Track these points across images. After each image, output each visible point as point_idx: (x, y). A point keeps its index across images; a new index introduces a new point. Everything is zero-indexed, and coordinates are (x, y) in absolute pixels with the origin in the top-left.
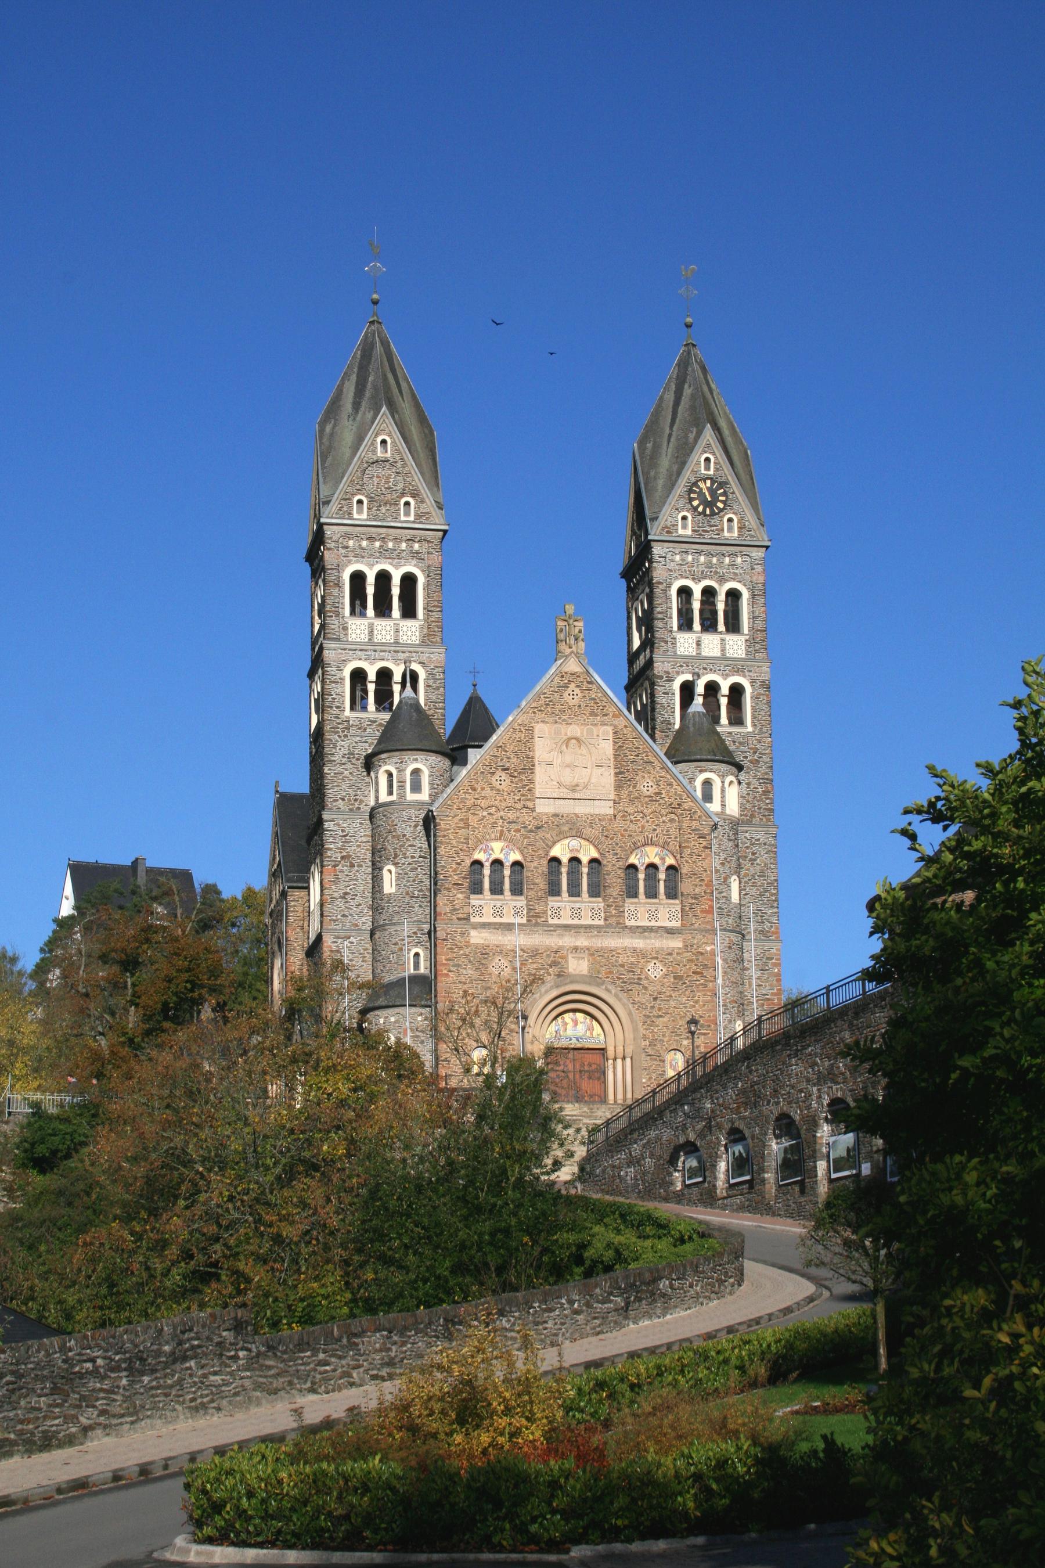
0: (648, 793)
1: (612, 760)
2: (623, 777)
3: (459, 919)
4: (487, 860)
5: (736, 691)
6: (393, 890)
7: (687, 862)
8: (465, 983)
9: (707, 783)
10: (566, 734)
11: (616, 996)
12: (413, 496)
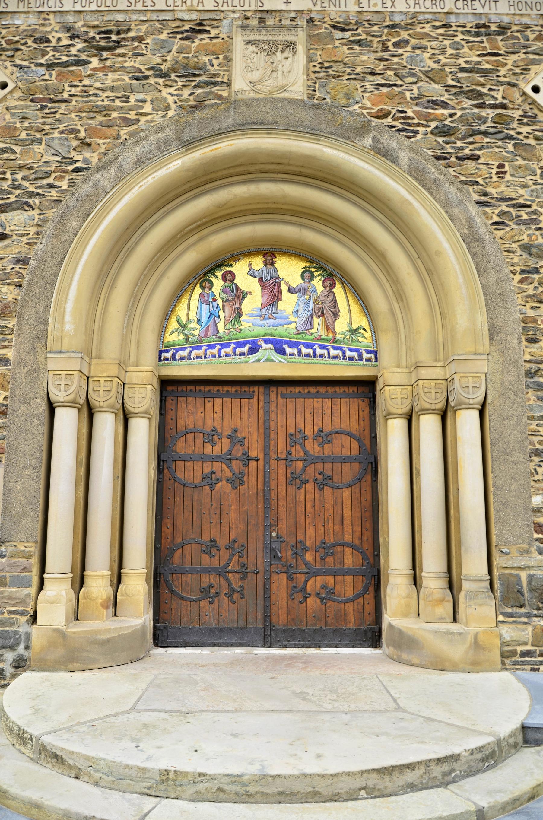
11: (417, 173)
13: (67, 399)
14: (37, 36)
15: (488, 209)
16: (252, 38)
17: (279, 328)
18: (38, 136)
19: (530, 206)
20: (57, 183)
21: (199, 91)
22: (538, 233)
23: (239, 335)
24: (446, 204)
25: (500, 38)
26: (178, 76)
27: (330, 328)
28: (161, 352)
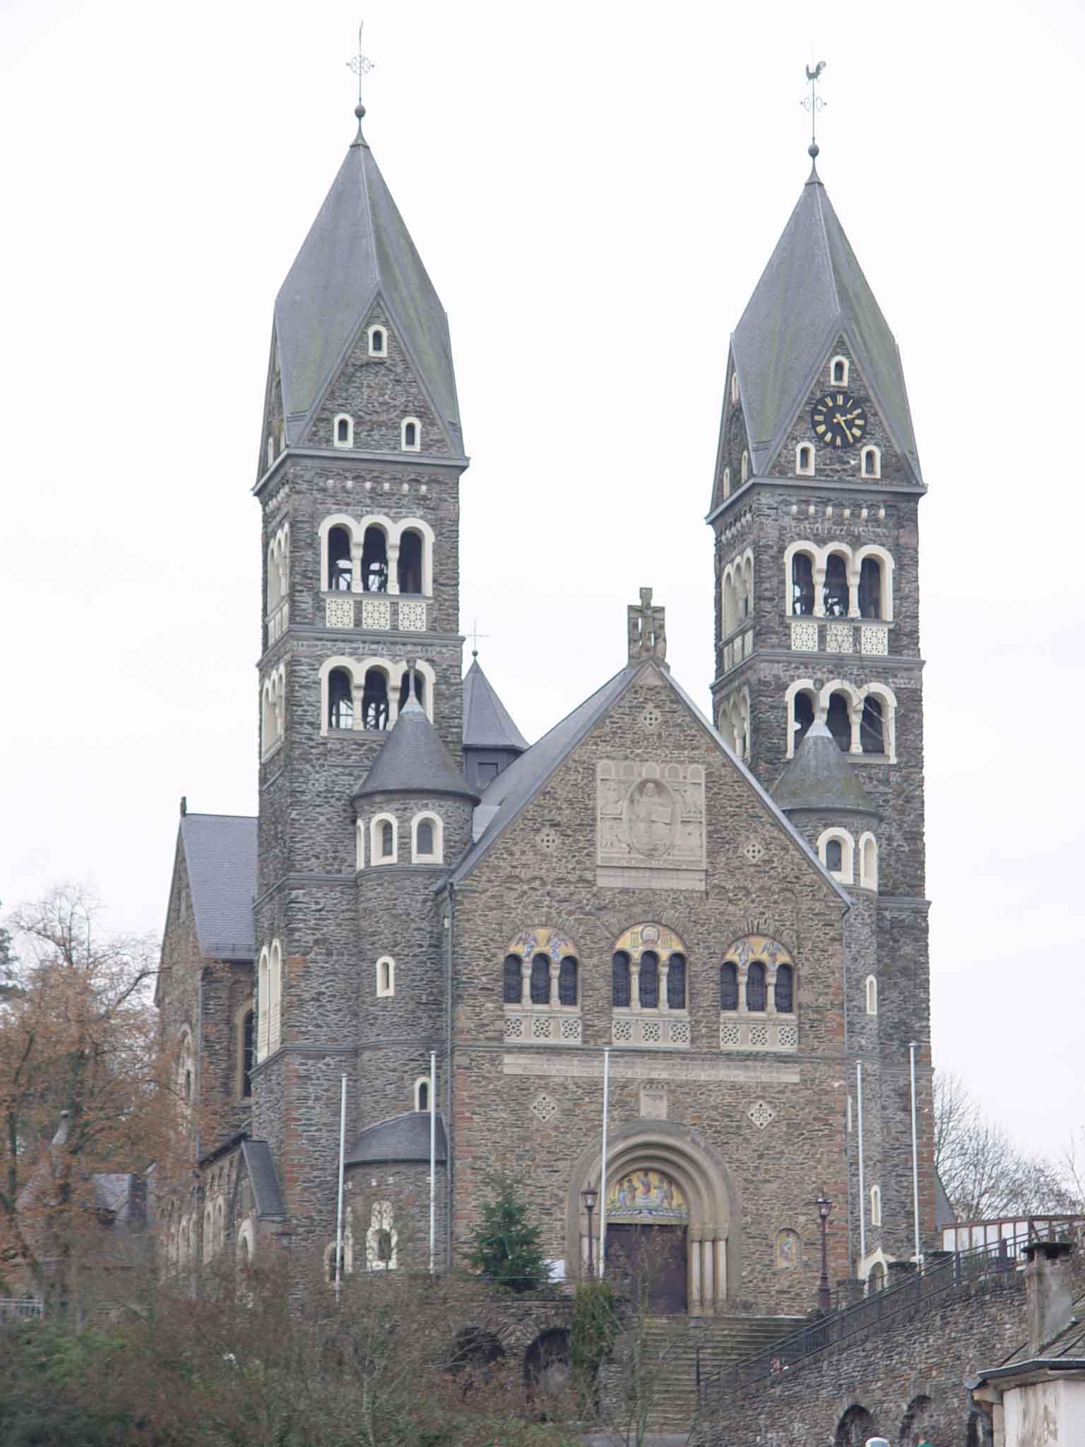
0: (754, 861)
1: (704, 812)
2: (719, 840)
3: (488, 1039)
4: (528, 954)
5: (874, 705)
6: (391, 992)
7: (807, 960)
8: (496, 1132)
9: (835, 845)
10: (640, 775)
11: (706, 1150)
12: (420, 416)
27: (670, 1204)
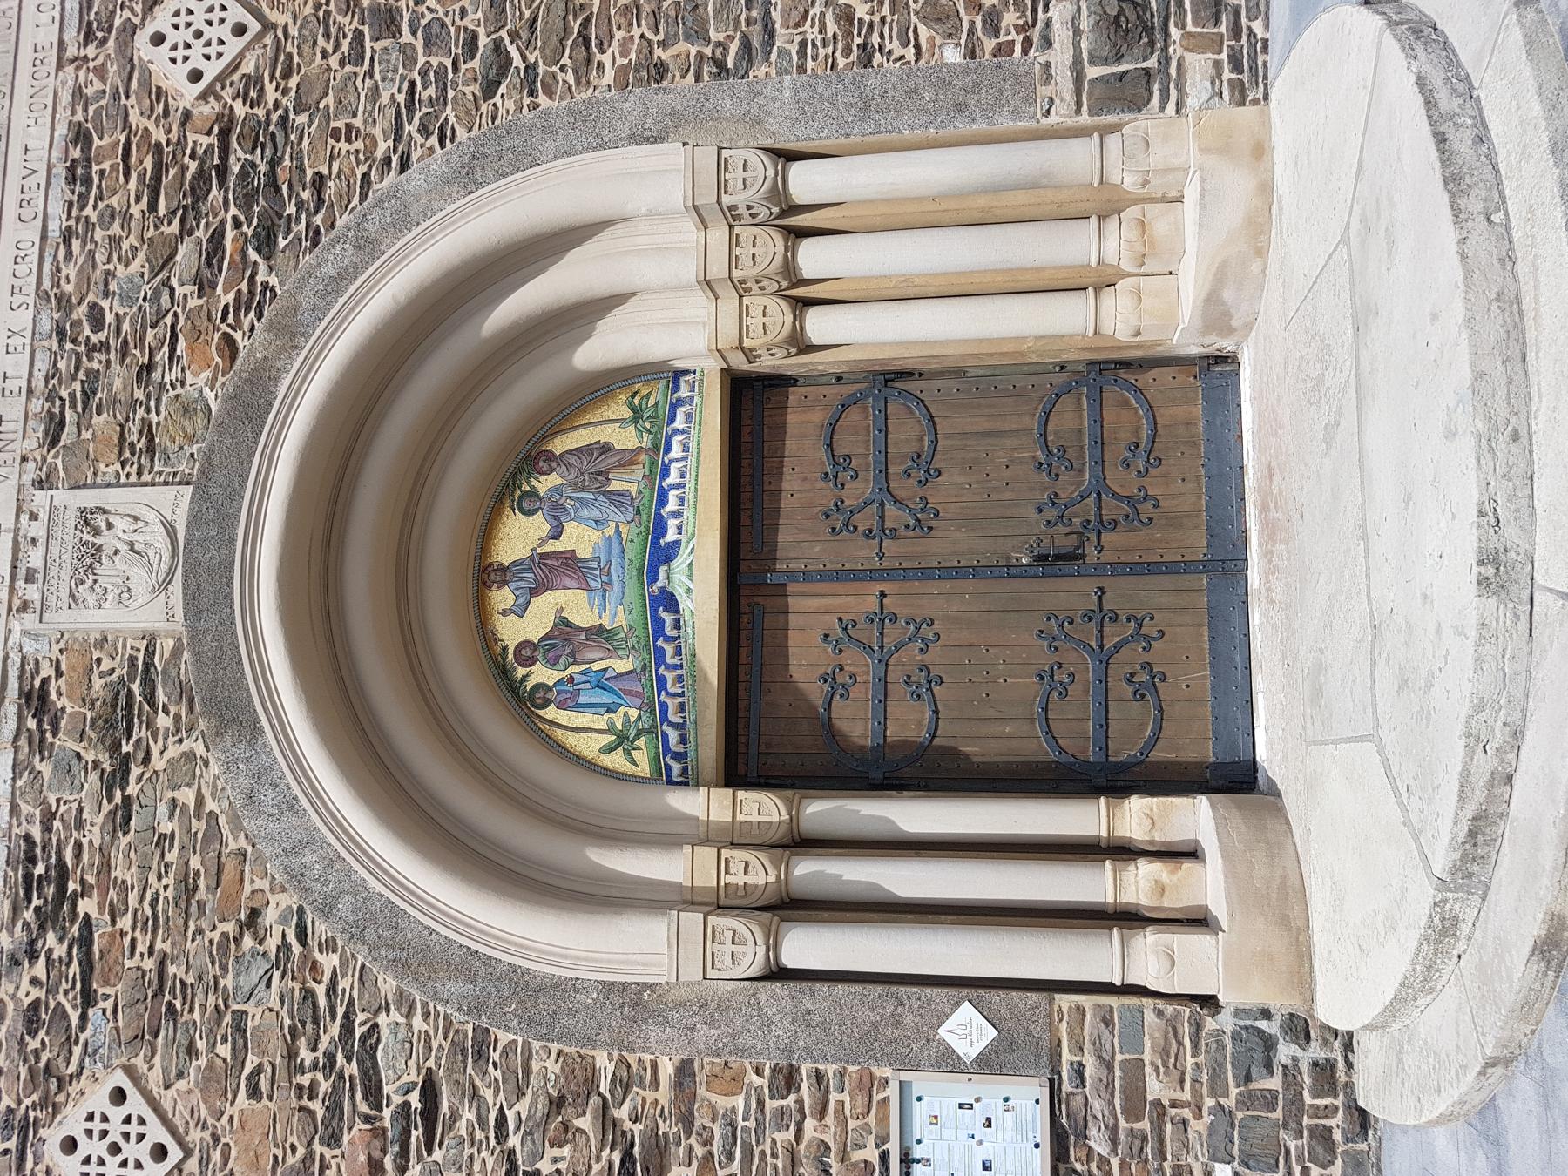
13: (760, 941)
14: (21, 1028)
15: (414, 156)
16: (64, 593)
17: (629, 555)
18: (228, 1019)
19: (412, 84)
20: (326, 979)
21: (162, 698)
22: (463, 67)
23: (640, 632)
24: (402, 223)
25: (97, 142)
26: (128, 740)
27: (628, 460)
28: (670, 782)
